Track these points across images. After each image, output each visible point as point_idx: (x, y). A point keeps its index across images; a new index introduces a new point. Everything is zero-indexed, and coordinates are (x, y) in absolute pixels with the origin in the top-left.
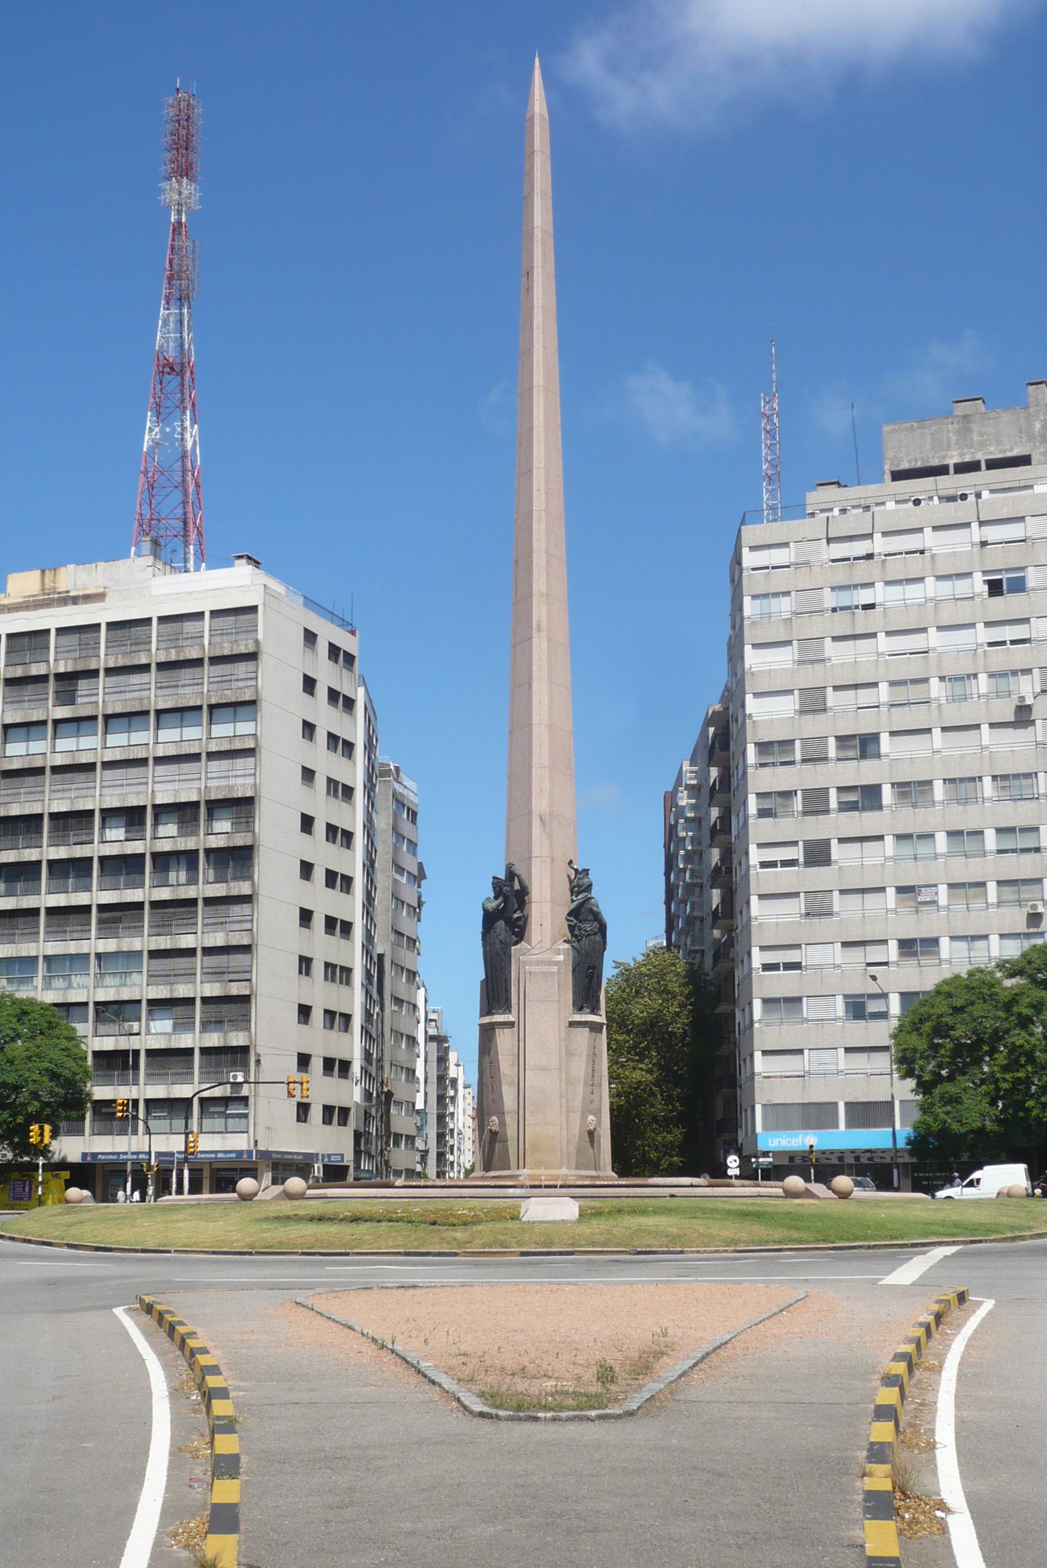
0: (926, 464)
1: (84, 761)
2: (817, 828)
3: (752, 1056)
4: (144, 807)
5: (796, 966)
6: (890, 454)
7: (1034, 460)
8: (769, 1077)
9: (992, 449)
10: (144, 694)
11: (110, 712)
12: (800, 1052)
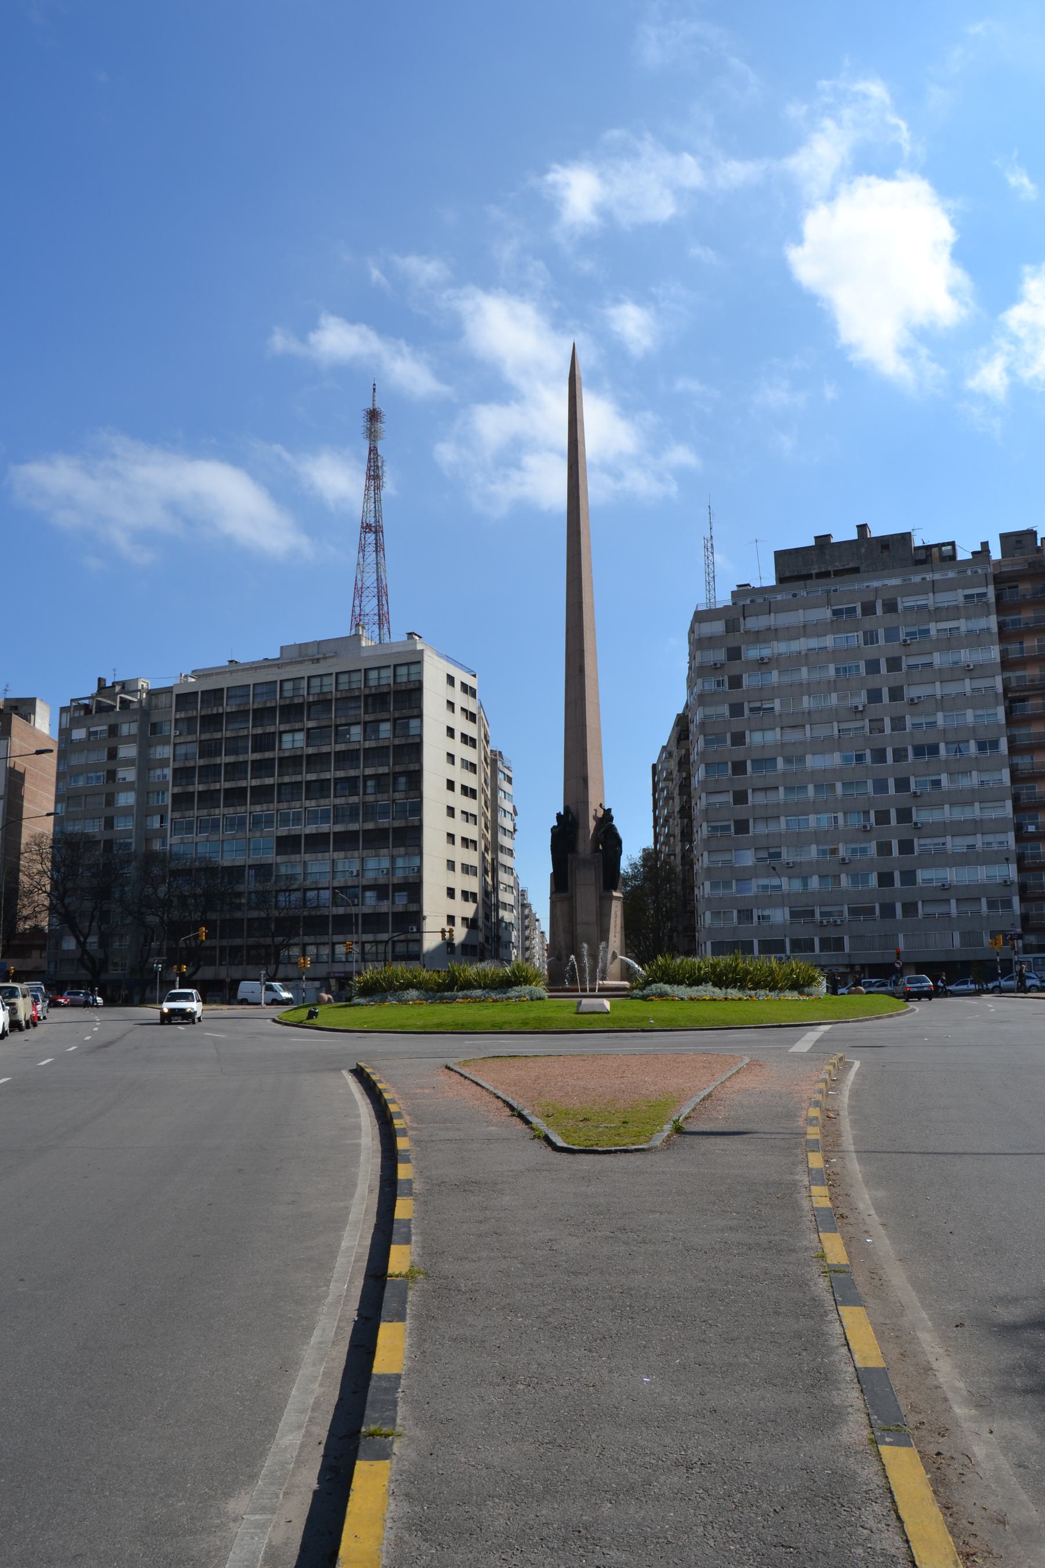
7: (862, 569)
10: (357, 712)
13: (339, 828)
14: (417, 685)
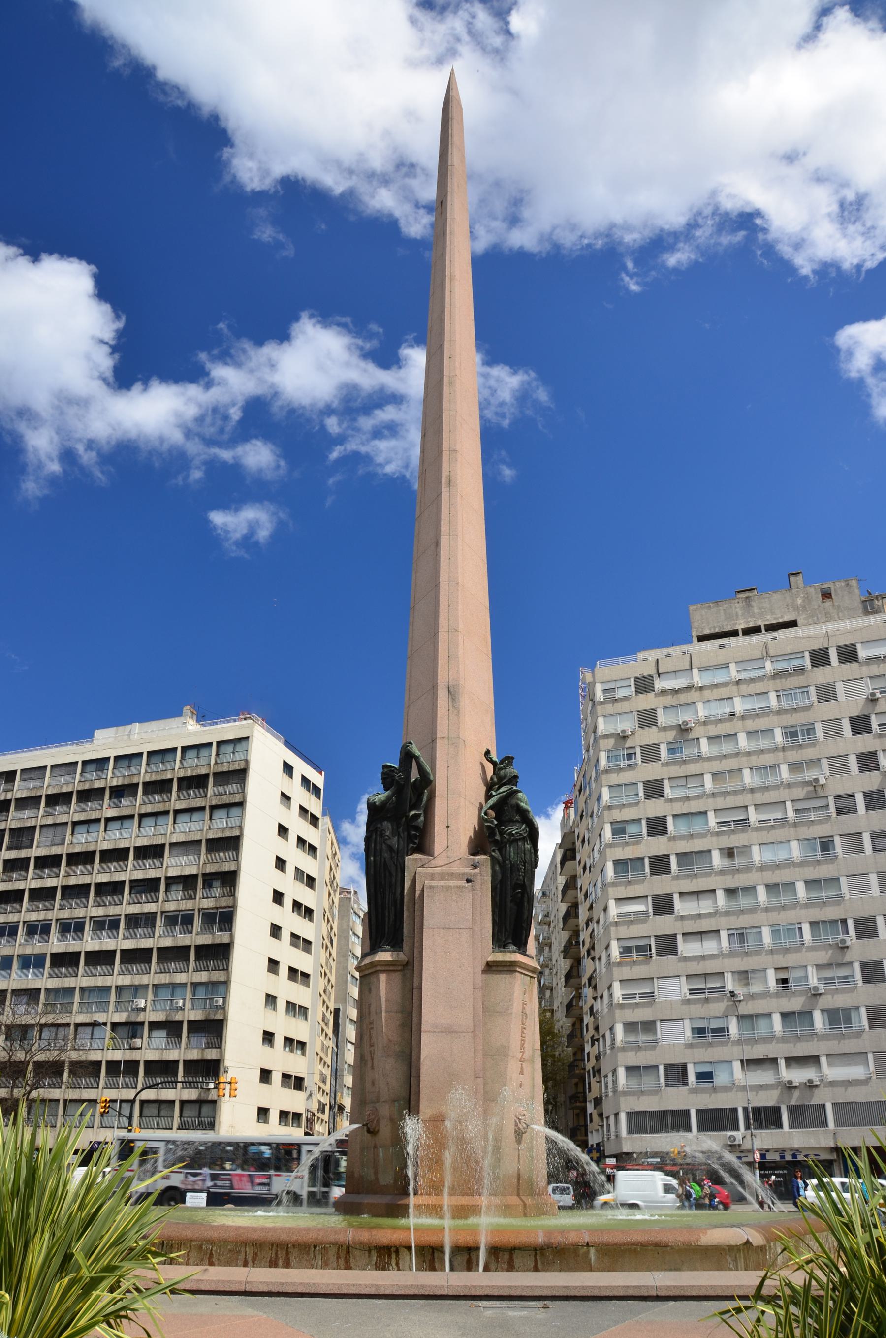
0: (722, 630)
1: (122, 846)
2: (661, 885)
4: (160, 879)
6: (696, 624)
7: (799, 623)
9: (768, 617)
11: (143, 812)
13: (129, 944)
14: (242, 766)
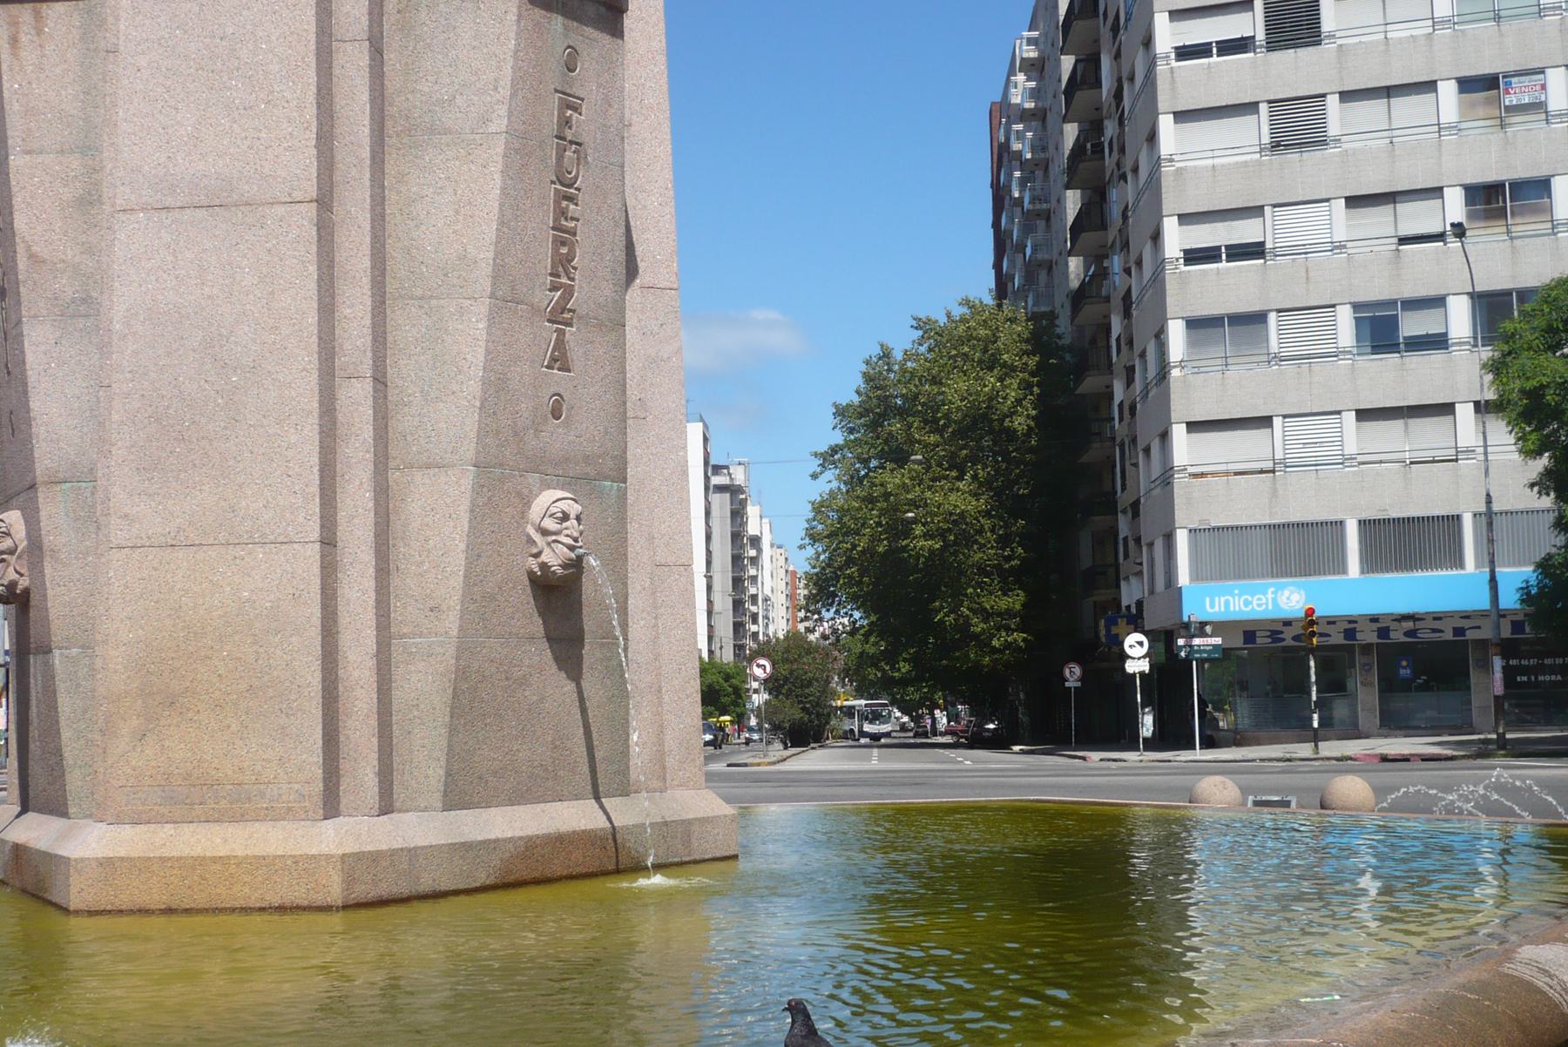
3: (1165, 436)
5: (1254, 251)
8: (1202, 475)
12: (1265, 422)
